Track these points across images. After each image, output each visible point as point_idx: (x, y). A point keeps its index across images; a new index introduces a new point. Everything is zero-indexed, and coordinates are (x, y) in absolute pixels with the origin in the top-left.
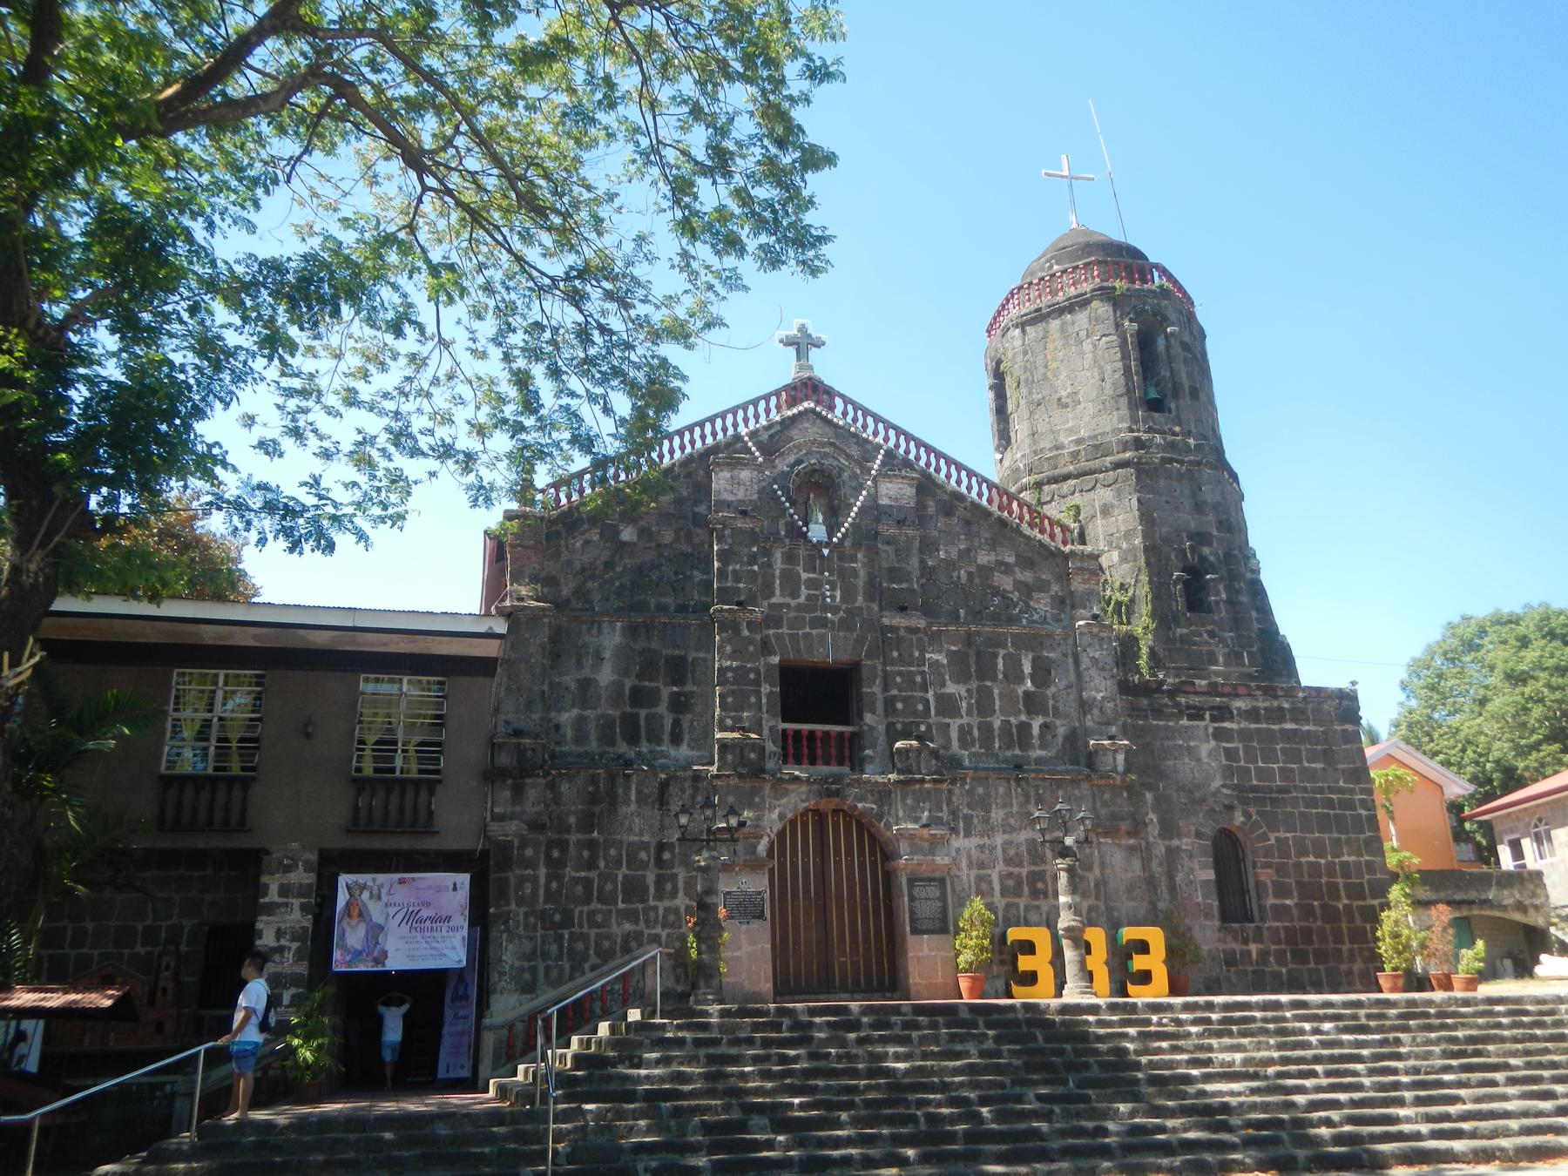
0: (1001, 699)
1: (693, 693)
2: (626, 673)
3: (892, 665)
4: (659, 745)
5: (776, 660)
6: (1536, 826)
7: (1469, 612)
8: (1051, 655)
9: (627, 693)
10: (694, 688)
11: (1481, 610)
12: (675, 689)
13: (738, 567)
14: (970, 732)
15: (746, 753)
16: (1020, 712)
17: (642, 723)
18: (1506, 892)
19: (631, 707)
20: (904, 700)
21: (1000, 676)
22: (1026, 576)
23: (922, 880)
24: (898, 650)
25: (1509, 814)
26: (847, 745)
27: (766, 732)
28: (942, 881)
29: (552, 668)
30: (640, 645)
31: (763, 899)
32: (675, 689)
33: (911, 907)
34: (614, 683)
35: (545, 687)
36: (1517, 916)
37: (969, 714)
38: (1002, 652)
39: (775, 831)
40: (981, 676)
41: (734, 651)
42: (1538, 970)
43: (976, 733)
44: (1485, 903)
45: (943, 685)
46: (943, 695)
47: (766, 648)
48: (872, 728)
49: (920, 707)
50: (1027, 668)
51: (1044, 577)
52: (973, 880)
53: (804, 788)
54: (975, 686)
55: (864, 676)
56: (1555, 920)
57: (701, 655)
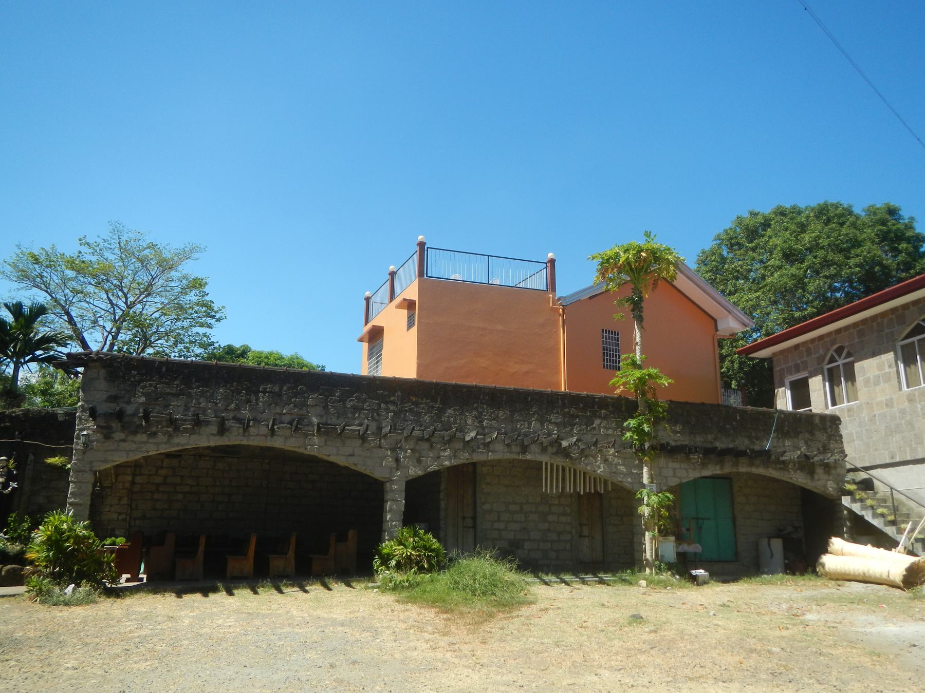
6: (832, 360)
7: (756, 211)
11: (766, 208)
18: (788, 443)
25: (797, 347)
36: (799, 479)
42: (829, 562)
44: (765, 456)
56: (852, 487)
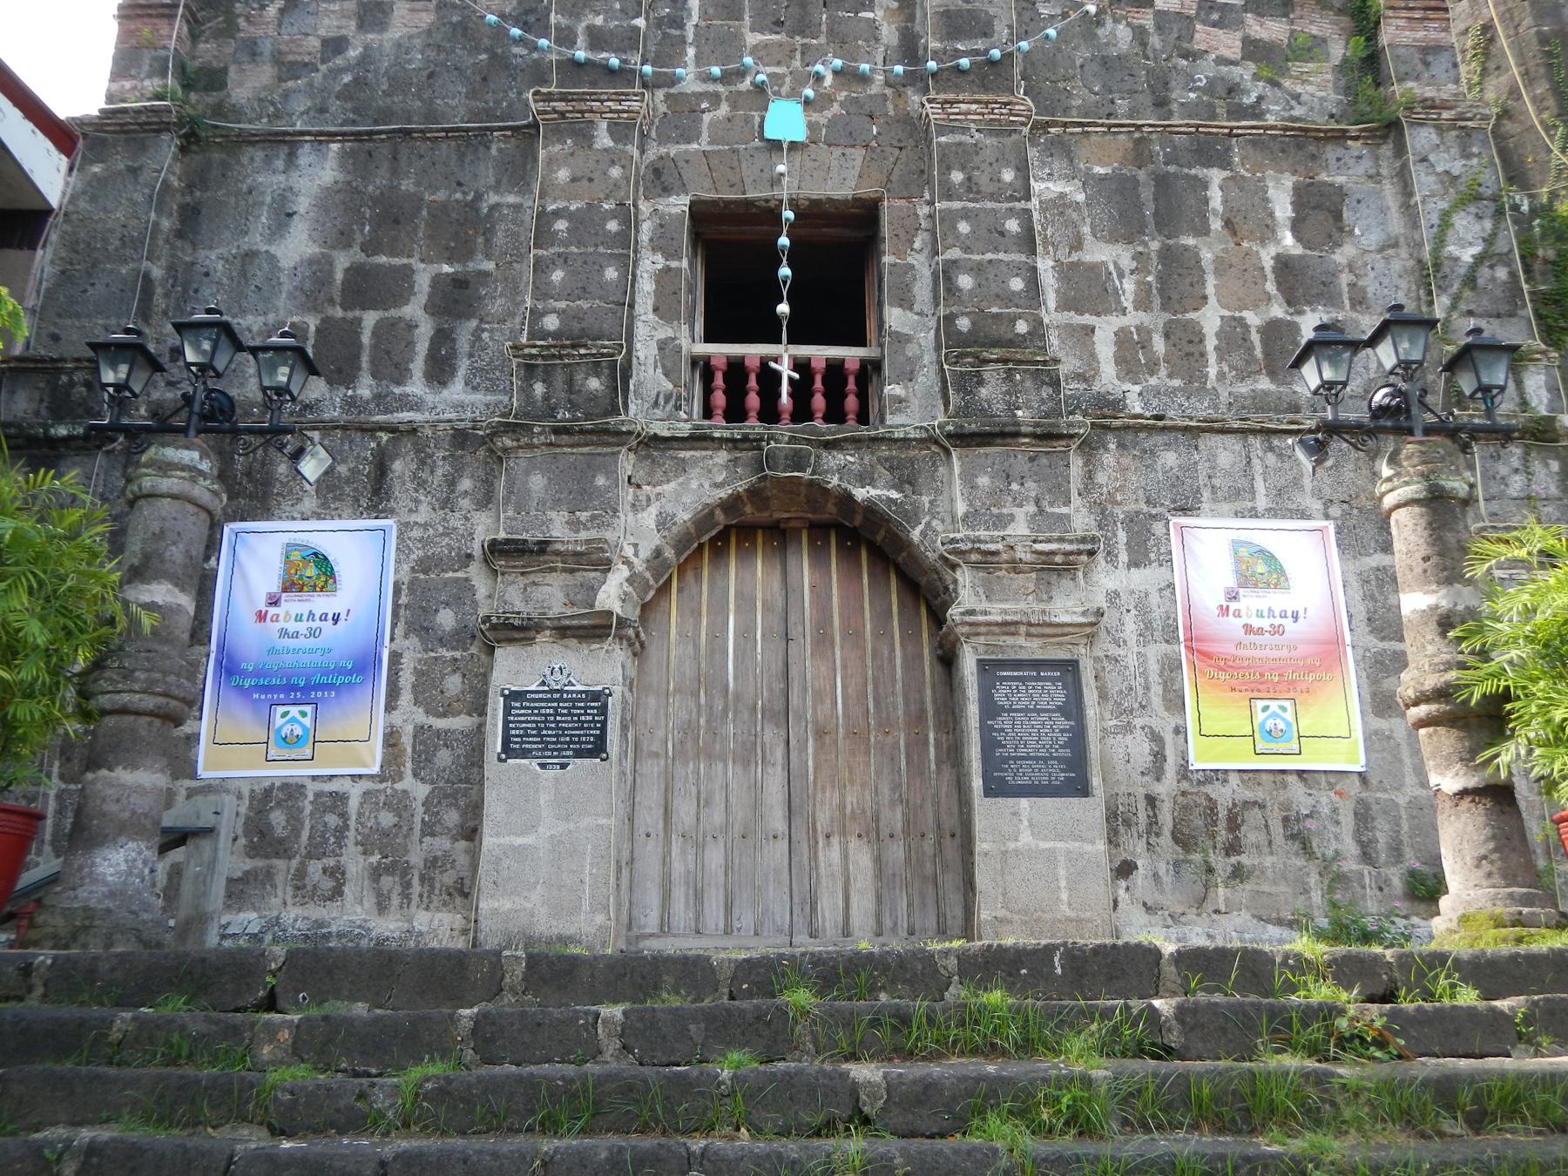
0: (1218, 272)
1: (487, 274)
2: (344, 239)
3: (949, 198)
4: (399, 383)
5: (678, 204)
8: (1340, 179)
9: (339, 276)
10: (489, 266)
12: (447, 269)
13: (599, 21)
14: (1145, 345)
15: (579, 377)
16: (1269, 298)
17: (366, 339)
19: (345, 310)
20: (977, 270)
21: (1216, 225)
22: (1271, 30)
23: (1018, 664)
24: (963, 168)
26: (851, 385)
27: (645, 351)
28: (1070, 668)
29: (180, 234)
30: (380, 180)
31: (603, 710)
32: (447, 269)
33: (985, 730)
34: (311, 262)
35: (157, 272)
37: (1142, 304)
38: (1216, 176)
39: (645, 552)
40: (1167, 222)
41: (574, 180)
43: (1159, 345)
45: (1077, 245)
46: (1075, 265)
47: (660, 179)
48: (901, 339)
49: (1017, 284)
50: (1283, 208)
51: (1314, 30)
52: (1154, 667)
53: (722, 456)
54: (1155, 245)
55: (886, 230)
57: (511, 199)
